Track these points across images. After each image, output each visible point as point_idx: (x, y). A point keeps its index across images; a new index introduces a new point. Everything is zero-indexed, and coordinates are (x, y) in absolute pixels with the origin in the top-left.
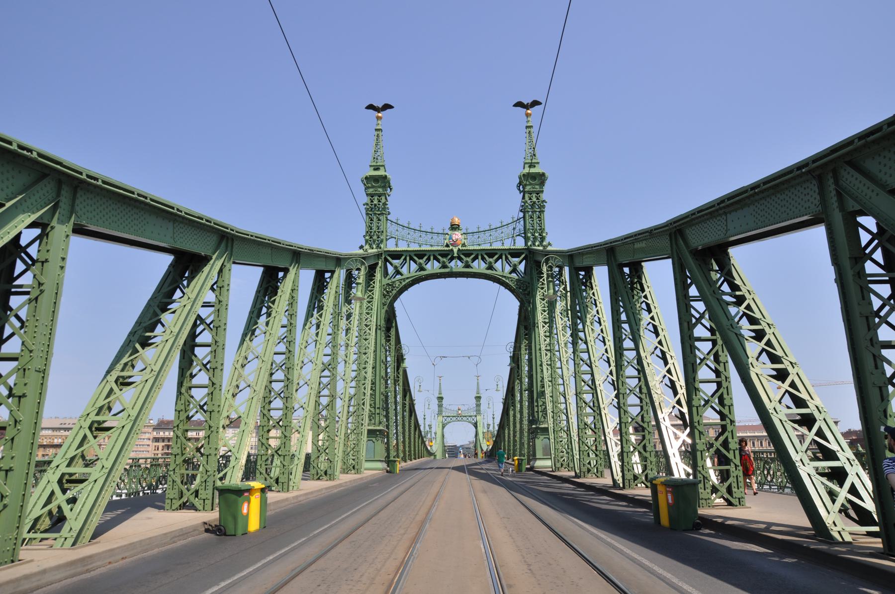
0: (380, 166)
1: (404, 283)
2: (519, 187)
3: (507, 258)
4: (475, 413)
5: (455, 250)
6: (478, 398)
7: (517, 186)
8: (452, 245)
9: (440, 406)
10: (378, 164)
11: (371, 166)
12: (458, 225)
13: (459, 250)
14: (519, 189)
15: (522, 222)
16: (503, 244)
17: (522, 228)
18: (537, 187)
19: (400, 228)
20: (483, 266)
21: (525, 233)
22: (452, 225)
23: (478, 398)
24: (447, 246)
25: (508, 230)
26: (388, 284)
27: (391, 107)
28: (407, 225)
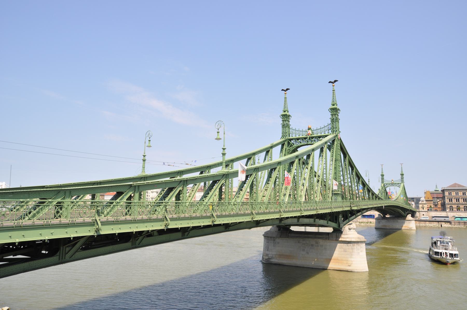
1: (293, 149)
4: (401, 182)
6: (402, 175)
8: (308, 135)
9: (383, 179)
11: (283, 111)
12: (310, 128)
18: (335, 112)
23: (402, 175)
24: (306, 135)
25: (326, 128)
26: (289, 149)
27: (289, 89)
28: (295, 129)
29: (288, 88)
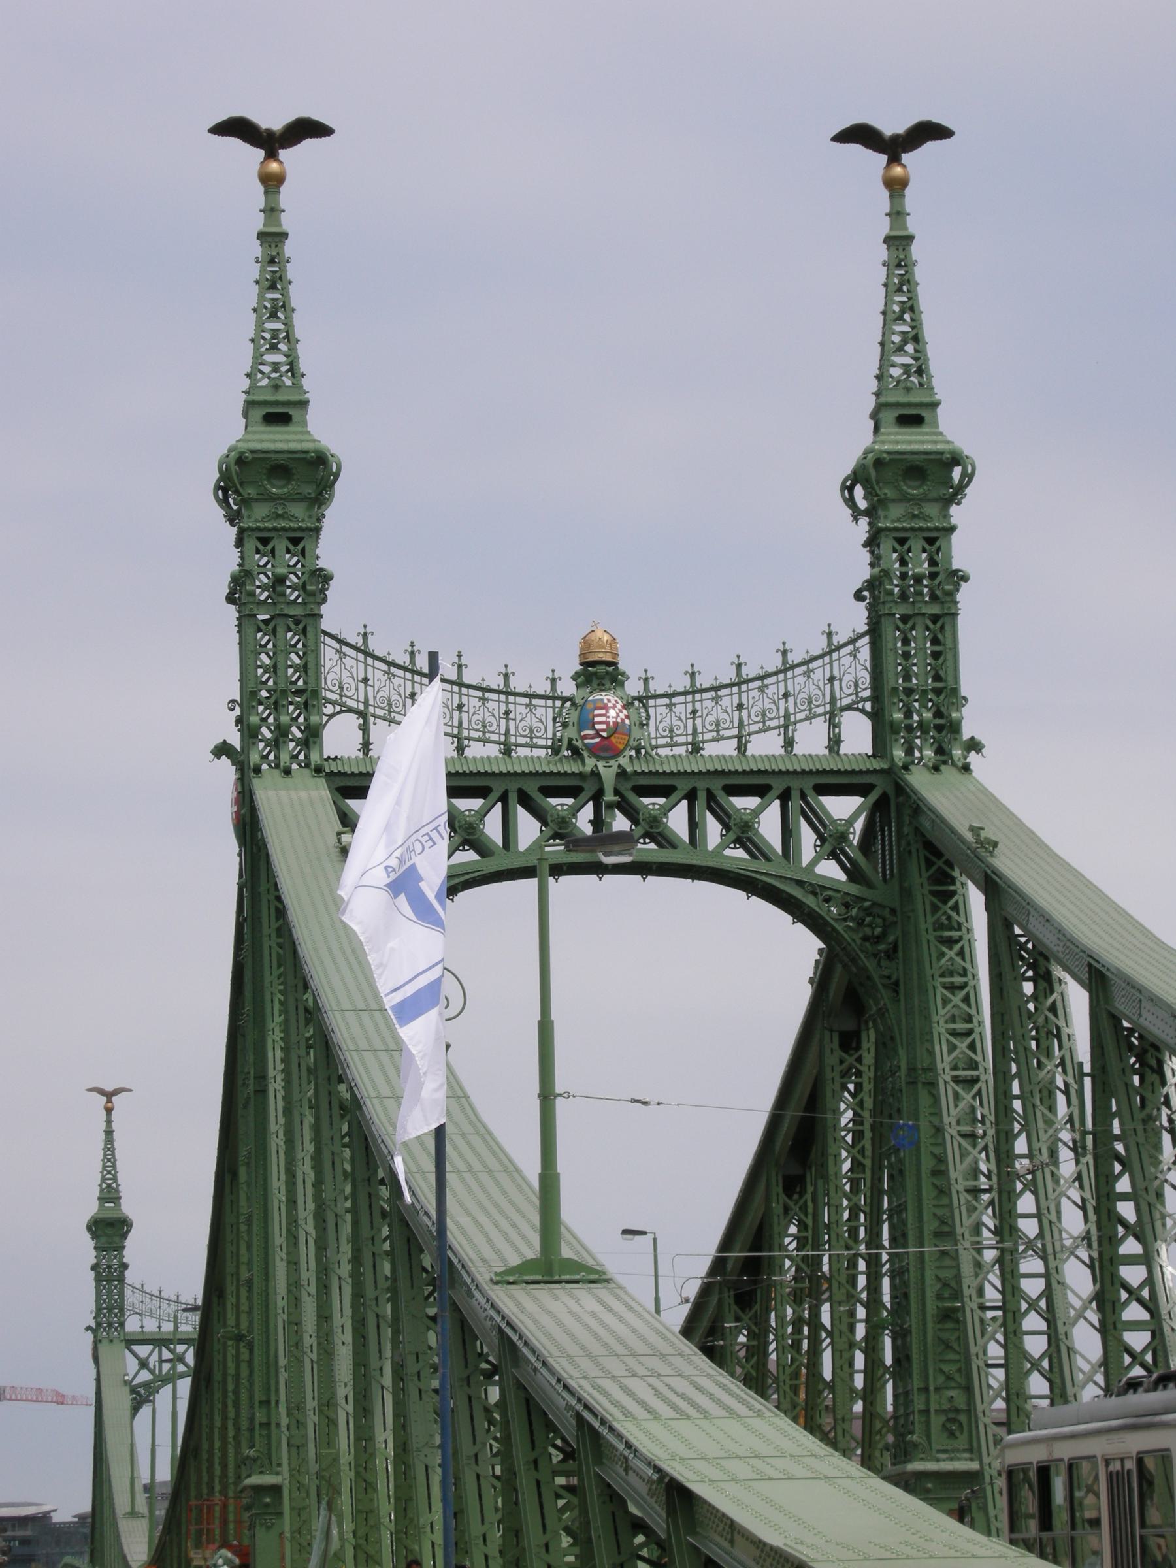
0: (289, 403)
2: (851, 489)
3: (803, 797)
5: (608, 774)
7: (844, 487)
8: (594, 751)
10: (281, 397)
13: (622, 774)
14: (851, 502)
15: (865, 654)
16: (789, 743)
17: (865, 677)
18: (932, 510)
19: (377, 673)
20: (713, 829)
21: (876, 698)
22: (586, 664)
29: (316, 117)
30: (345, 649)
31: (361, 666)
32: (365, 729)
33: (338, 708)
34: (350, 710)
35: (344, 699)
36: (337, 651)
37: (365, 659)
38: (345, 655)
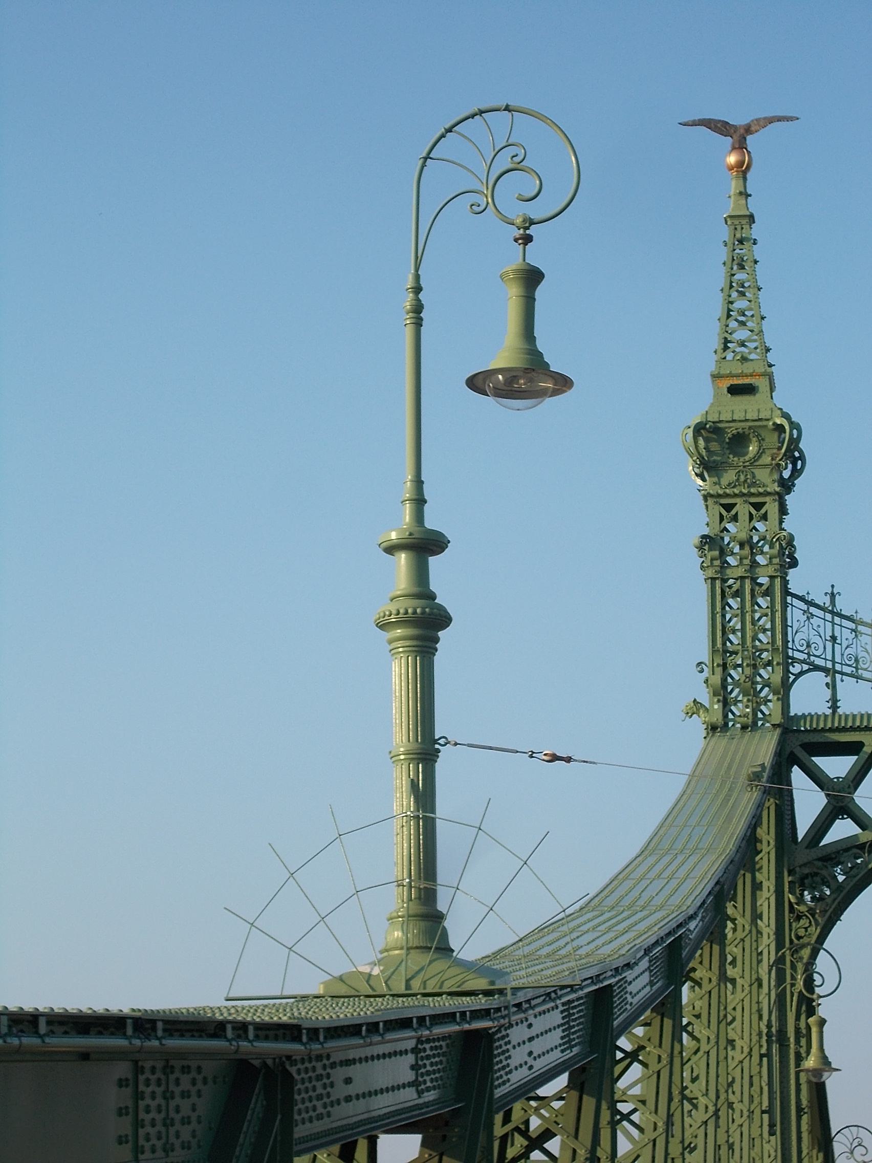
10: (748, 368)
30: (812, 609)
31: (829, 625)
32: (833, 686)
33: (806, 667)
34: (817, 668)
35: (812, 658)
36: (805, 611)
37: (833, 618)
38: (812, 615)
